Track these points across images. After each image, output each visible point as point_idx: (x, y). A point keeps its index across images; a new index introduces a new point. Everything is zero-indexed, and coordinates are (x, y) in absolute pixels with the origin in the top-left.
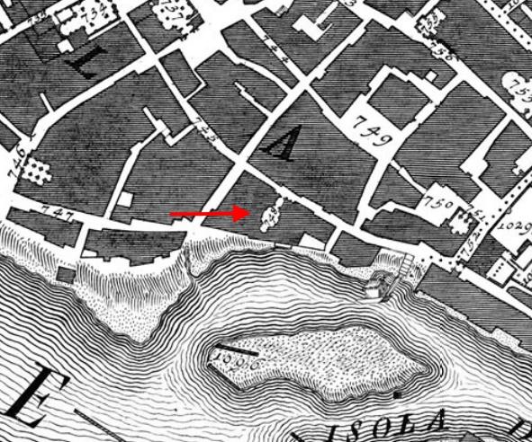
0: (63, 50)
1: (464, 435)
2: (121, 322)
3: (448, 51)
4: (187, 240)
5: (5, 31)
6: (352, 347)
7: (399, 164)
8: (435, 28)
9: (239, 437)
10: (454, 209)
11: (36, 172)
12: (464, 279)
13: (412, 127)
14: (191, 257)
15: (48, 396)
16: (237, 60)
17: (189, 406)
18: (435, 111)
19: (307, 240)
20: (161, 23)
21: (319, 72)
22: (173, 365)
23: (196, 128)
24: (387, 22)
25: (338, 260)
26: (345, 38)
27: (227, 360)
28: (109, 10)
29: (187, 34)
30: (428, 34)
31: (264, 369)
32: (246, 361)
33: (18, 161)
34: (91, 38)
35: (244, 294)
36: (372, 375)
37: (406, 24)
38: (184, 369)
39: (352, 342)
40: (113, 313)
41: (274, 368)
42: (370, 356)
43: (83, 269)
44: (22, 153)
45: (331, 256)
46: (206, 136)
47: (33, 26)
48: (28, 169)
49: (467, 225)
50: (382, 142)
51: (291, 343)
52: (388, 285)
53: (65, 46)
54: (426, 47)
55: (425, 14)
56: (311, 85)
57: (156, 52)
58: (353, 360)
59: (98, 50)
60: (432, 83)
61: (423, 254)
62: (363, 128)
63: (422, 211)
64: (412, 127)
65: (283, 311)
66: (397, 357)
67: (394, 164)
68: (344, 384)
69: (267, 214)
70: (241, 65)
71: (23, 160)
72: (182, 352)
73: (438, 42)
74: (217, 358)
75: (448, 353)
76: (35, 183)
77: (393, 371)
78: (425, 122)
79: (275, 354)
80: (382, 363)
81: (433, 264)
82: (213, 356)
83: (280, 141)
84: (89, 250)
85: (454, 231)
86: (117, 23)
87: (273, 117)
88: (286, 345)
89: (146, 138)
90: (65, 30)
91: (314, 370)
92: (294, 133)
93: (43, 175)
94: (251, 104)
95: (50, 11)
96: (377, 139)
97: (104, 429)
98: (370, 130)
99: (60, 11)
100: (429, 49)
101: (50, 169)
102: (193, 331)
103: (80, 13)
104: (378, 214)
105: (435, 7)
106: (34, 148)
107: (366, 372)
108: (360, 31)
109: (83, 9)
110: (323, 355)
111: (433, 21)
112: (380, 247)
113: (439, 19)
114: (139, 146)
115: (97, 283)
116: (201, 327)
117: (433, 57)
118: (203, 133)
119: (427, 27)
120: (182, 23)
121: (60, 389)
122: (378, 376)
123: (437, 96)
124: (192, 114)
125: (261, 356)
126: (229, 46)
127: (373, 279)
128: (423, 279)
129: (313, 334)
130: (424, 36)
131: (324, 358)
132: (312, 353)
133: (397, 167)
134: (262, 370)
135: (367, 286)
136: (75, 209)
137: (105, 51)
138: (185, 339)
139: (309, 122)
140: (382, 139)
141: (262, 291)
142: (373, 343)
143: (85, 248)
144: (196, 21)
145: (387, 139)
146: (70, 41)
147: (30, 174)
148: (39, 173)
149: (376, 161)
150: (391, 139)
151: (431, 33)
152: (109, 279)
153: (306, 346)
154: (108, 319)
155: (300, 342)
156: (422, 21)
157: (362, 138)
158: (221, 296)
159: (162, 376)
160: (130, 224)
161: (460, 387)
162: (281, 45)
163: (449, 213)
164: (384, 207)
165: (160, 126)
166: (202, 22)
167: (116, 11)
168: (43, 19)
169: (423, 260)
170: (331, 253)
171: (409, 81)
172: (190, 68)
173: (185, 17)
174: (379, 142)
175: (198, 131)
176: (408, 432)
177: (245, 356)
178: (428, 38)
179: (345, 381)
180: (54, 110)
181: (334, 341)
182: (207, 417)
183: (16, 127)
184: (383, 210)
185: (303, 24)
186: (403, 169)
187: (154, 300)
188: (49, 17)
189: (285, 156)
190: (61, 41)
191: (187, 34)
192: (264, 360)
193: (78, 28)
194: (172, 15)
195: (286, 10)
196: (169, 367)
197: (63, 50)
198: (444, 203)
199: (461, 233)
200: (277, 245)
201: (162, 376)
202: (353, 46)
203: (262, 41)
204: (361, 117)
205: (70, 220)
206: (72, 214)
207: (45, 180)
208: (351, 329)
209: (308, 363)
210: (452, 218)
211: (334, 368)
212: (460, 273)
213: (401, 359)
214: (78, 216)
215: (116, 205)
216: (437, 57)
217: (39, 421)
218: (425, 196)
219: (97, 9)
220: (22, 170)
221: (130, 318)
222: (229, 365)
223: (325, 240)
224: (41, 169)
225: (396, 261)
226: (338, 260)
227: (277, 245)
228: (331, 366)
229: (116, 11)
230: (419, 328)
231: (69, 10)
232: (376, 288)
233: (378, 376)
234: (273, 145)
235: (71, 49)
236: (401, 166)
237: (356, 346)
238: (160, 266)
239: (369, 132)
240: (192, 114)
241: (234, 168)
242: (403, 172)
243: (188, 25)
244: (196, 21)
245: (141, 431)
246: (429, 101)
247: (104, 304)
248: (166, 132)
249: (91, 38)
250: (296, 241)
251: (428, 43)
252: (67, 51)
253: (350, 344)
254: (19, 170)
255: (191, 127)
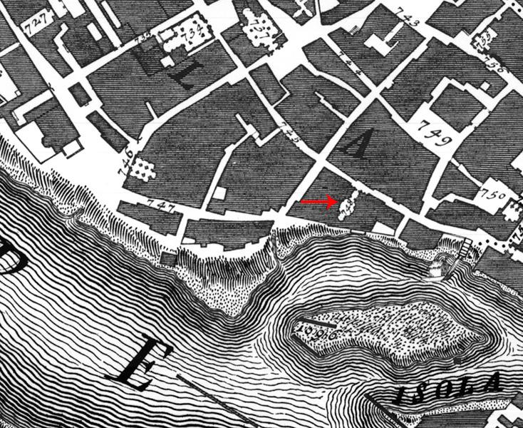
0: (165, 65)
1: (516, 395)
2: (217, 299)
3: (499, 64)
4: (274, 227)
5: (116, 49)
6: (418, 320)
7: (458, 161)
8: (488, 44)
9: (320, 398)
10: (506, 200)
11: (142, 170)
12: (515, 260)
13: (468, 130)
14: (278, 242)
15: (153, 363)
16: (317, 73)
17: (276, 371)
18: (489, 116)
19: (380, 228)
20: (250, 41)
21: (388, 83)
22: (262, 336)
23: (282, 131)
24: (445, 39)
25: (406, 244)
26: (410, 53)
27: (309, 331)
28: (205, 31)
29: (273, 51)
30: (482, 50)
31: (341, 339)
32: (325, 331)
33: (126, 161)
34: (189, 55)
35: (324, 274)
36: (435, 344)
37: (462, 41)
38: (271, 340)
39: (418, 315)
40: (210, 292)
41: (350, 338)
42: (433, 327)
43: (183, 253)
44: (130, 154)
45: (400, 241)
46: (291, 138)
47: (139, 44)
48: (135, 168)
49: (518, 213)
50: (443, 143)
51: (365, 317)
52: (449, 265)
53: (167, 61)
54: (481, 61)
55: (479, 33)
56: (381, 94)
57: (246, 65)
58: (419, 330)
59: (196, 65)
60: (486, 92)
61: (479, 238)
62: (427, 130)
63: (479, 201)
64: (468, 130)
65: (357, 289)
66: (457, 328)
67: (454, 161)
68: (411, 351)
69: (343, 206)
70: (320, 76)
71: (131, 160)
72: (268, 326)
73: (491, 57)
74: (300, 330)
75: (501, 323)
76: (142, 180)
77: (454, 339)
78: (480, 125)
79: (351, 326)
80: (443, 333)
81: (488, 247)
82: (296, 329)
83: (355, 142)
84: (188, 237)
85: (506, 219)
86: (213, 41)
87: (348, 121)
88: (360, 318)
89: (238, 140)
90: (168, 48)
91: (384, 340)
92: (368, 135)
93: (149, 173)
94: (330, 110)
95: (154, 32)
96: (439, 140)
97: (202, 392)
98: (432, 132)
99: (163, 32)
100: (484, 63)
101: (155, 167)
102: (278, 305)
103: (180, 33)
104: (440, 204)
105: (488, 26)
106: (141, 150)
107: (430, 340)
108: (422, 47)
109: (182, 30)
110: (392, 326)
111: (487, 39)
112: (442, 233)
113: (492, 37)
114: (232, 147)
115: (194, 264)
116: (286, 303)
117: (487, 69)
118: (288, 135)
119: (482, 44)
120: (268, 41)
121: (164, 357)
122: (440, 344)
123: (490, 103)
124: (278, 119)
125: (338, 328)
126: (310, 61)
127: (436, 260)
128: (480, 260)
129: (384, 308)
130: (479, 51)
131: (393, 329)
132: (383, 325)
133: (457, 164)
134: (339, 339)
135: (432, 267)
136: (176, 202)
137: (202, 66)
138: (272, 313)
139: (383, 127)
140: (443, 140)
141: (339, 271)
142: (437, 316)
143: (185, 236)
144: (281, 39)
145: (447, 140)
146: (171, 57)
147: (138, 172)
148: (145, 171)
149: (438, 159)
150: (451, 140)
151: (485, 49)
152: (205, 262)
153: (377, 319)
154: (205, 297)
155: (372, 316)
156: (477, 38)
157: (427, 139)
158: (303, 276)
159: (252, 346)
160: (224, 214)
161: (512, 353)
162: (353, 59)
163: (502, 203)
164: (446, 198)
165: (250, 130)
166: (287, 40)
167: (211, 31)
168: (148, 39)
169: (480, 244)
170: (399, 238)
171: (466, 91)
172: (276, 79)
173: (271, 36)
174: (440, 142)
175: (284, 134)
176: (467, 393)
177: (324, 328)
178: (482, 53)
179: (411, 349)
180: (158, 117)
181: (402, 314)
182: (292, 381)
183: (125, 131)
184: (445, 201)
185: (373, 42)
186: (462, 165)
187: (246, 281)
188: (154, 36)
189: (359, 154)
190: (164, 57)
191: (273, 51)
192: (341, 331)
193: (179, 45)
194: (259, 34)
195: (358, 29)
196: (259, 338)
197: (165, 65)
198: (498, 195)
199: (513, 220)
200: (353, 231)
201: (252, 346)
202: (417, 60)
203: (338, 57)
204: (424, 121)
205: (172, 212)
206: (173, 207)
207: (150, 178)
208: (417, 304)
209: (379, 334)
210: (505, 207)
211: (402, 338)
212: (512, 255)
213: (461, 330)
214: (179, 208)
215: (212, 198)
216: (491, 69)
217: (147, 384)
218: (481, 189)
219: (195, 30)
220: (130, 168)
221: (224, 295)
222: (310, 335)
223: (395, 227)
224: (147, 168)
225: (457, 244)
226: (406, 244)
227: (353, 231)
228: (399, 336)
229: (211, 31)
230: (477, 303)
231: (170, 30)
232: (439, 267)
233: (440, 344)
234: (350, 145)
235: (173, 64)
236: (460, 163)
237: (421, 318)
238: (249, 251)
239: (432, 134)
240: (278, 119)
241: (315, 166)
242: (462, 168)
243: (274, 43)
244: (281, 39)
245: (235, 393)
246: (483, 107)
247: (201, 284)
248: (256, 135)
249: (189, 55)
250: (370, 228)
251: (482, 57)
252: (170, 66)
253: (416, 317)
254: (127, 168)
255: (277, 131)
